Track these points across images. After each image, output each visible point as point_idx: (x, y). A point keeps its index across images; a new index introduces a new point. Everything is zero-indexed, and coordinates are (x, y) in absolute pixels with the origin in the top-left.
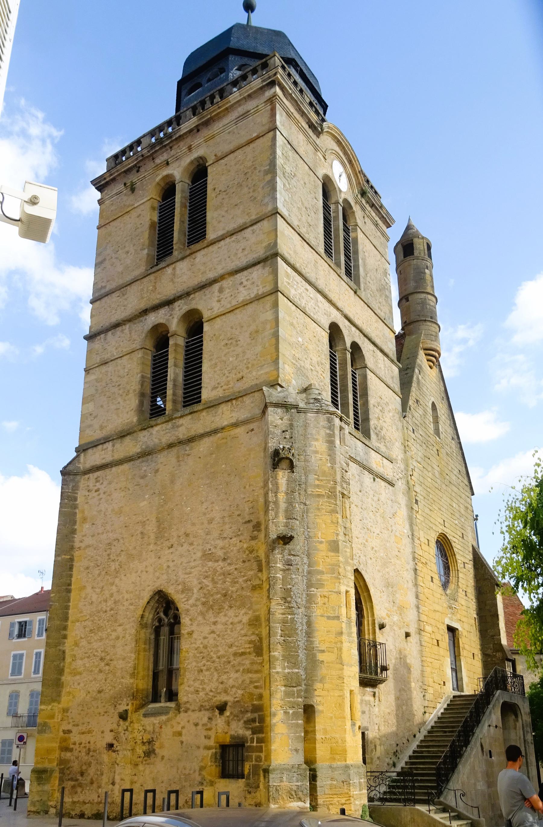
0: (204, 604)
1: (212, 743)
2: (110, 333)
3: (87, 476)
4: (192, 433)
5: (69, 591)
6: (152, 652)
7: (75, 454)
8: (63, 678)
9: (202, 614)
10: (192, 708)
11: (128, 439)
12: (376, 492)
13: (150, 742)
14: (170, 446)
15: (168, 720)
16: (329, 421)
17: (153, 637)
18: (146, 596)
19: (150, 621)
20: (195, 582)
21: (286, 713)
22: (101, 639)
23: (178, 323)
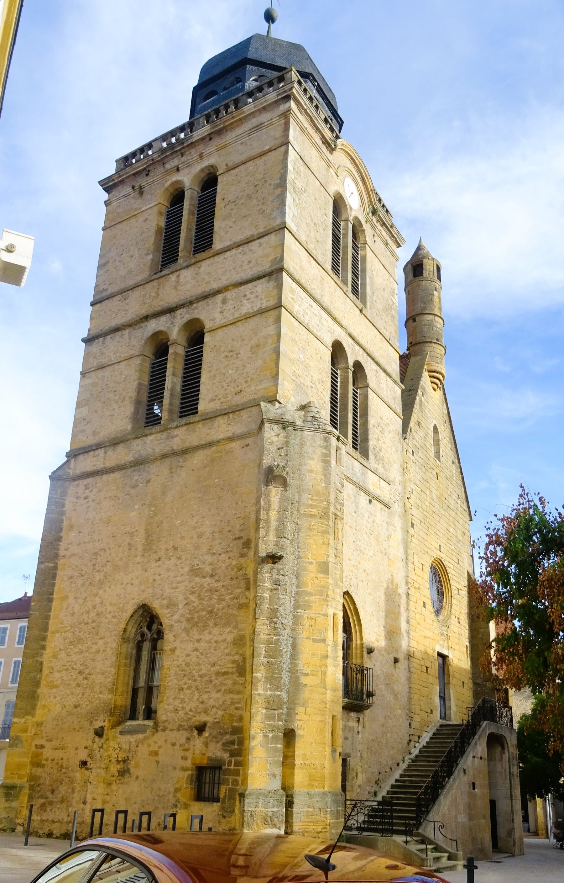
0: (188, 620)
1: (188, 764)
2: (109, 337)
3: (76, 483)
4: (187, 444)
5: (51, 600)
6: (132, 668)
7: (66, 459)
8: (39, 691)
9: (186, 631)
11: (120, 447)
12: (371, 514)
14: (164, 456)
15: (146, 738)
16: (326, 440)
17: (134, 652)
18: (130, 609)
19: (132, 635)
20: (181, 597)
21: (265, 736)
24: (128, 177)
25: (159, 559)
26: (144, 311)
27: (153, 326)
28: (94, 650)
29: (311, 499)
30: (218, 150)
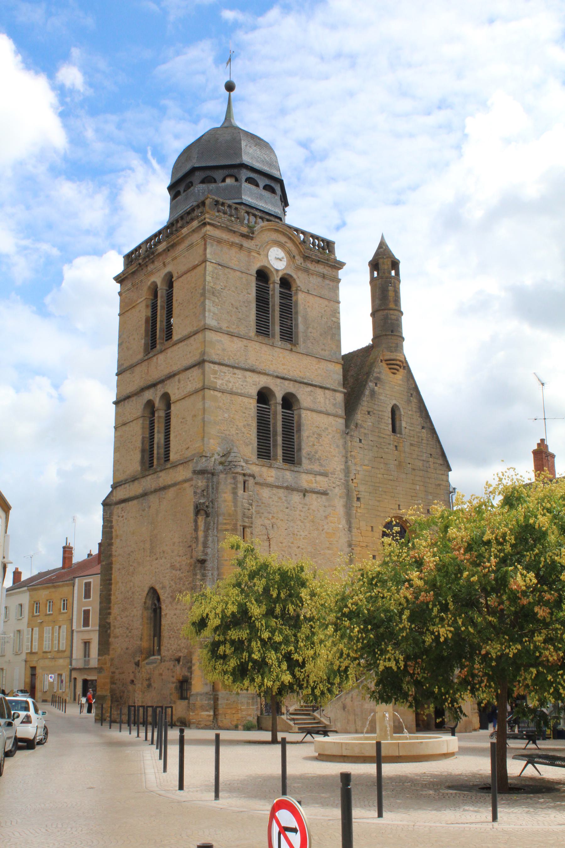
1: (174, 680)
2: (126, 401)
3: (117, 506)
4: (166, 484)
6: (152, 625)
9: (171, 603)
10: (166, 659)
11: (136, 482)
13: (149, 679)
14: (156, 491)
16: (234, 478)
17: (152, 615)
18: (146, 590)
19: (150, 606)
20: (167, 583)
22: (127, 616)
23: (159, 402)
24: (129, 275)
25: (156, 559)
26: (142, 384)
27: (148, 395)
28: (132, 615)
29: (226, 519)
30: (173, 260)
